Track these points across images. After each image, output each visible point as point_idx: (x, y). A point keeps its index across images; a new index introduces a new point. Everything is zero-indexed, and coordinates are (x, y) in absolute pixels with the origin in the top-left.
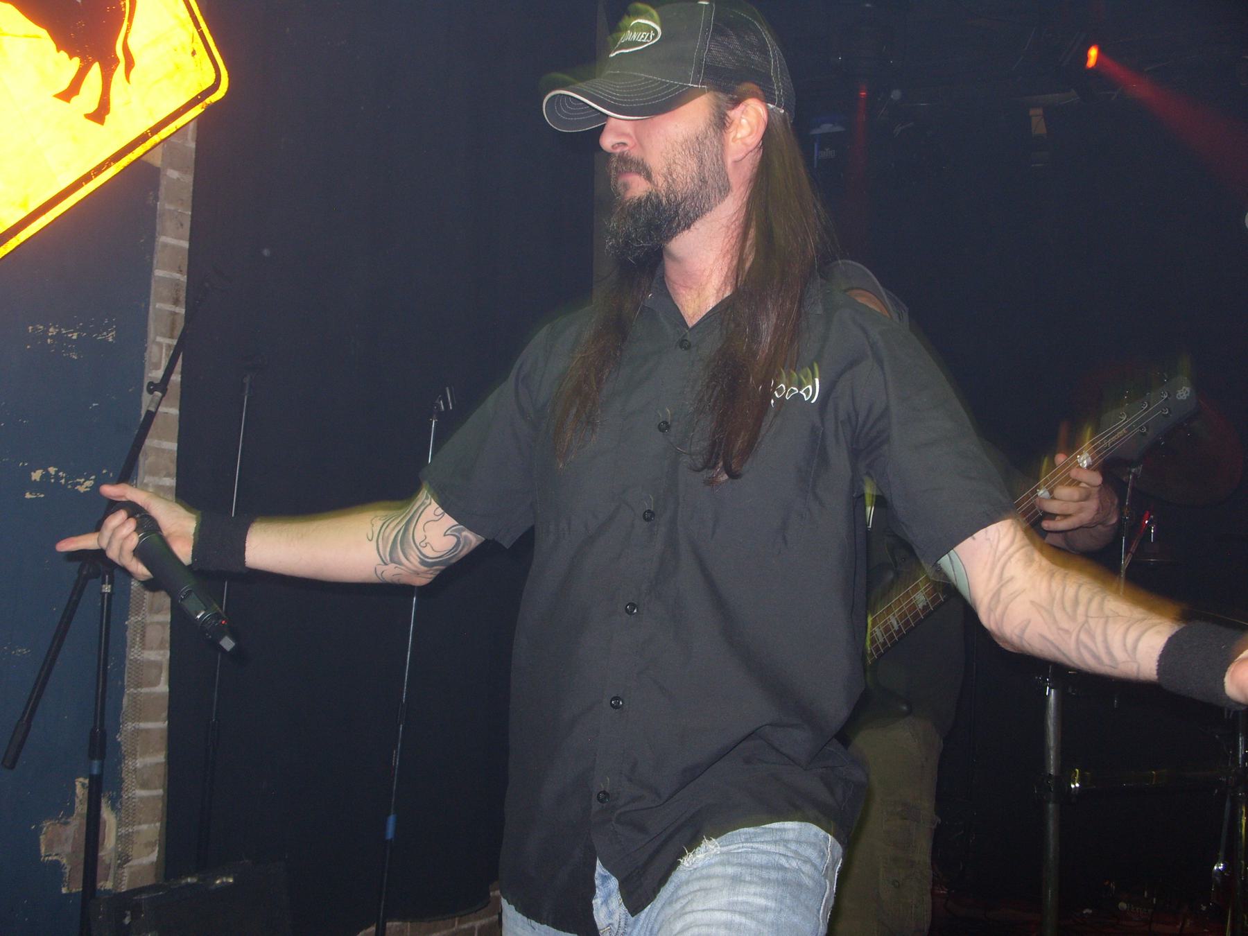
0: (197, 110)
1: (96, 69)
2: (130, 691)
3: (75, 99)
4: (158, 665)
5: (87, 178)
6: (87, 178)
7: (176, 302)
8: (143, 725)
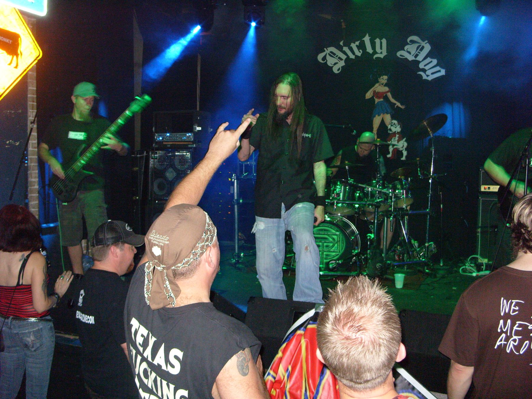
0: (36, 61)
1: (15, 57)
2: (29, 188)
3: (12, 64)
4: (35, 182)
5: (15, 81)
6: (15, 81)
7: (33, 102)
8: (32, 195)
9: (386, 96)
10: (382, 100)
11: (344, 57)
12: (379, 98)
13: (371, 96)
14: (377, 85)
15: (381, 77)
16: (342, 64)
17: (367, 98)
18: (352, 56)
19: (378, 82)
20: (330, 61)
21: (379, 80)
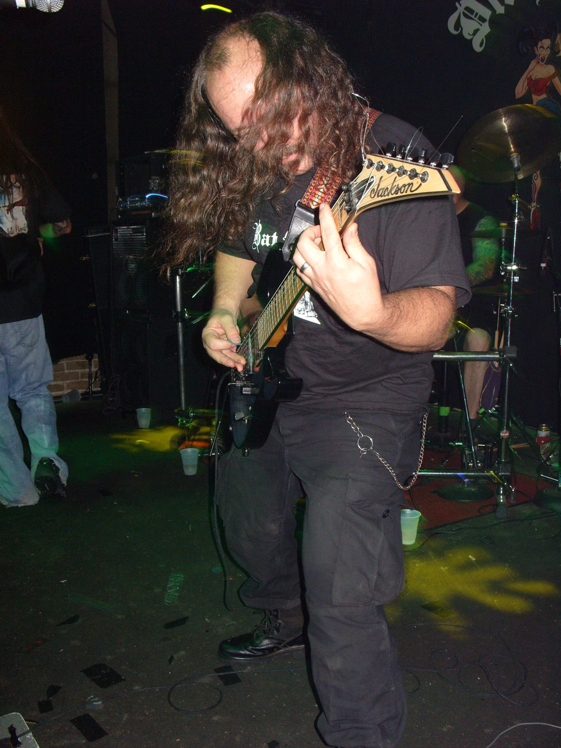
9: (552, 85)
10: (544, 96)
11: (486, 13)
12: (539, 93)
13: (524, 92)
14: (533, 63)
15: (539, 45)
16: (485, 29)
17: (518, 96)
18: (500, 10)
19: (534, 56)
20: (468, 27)
21: (537, 53)
